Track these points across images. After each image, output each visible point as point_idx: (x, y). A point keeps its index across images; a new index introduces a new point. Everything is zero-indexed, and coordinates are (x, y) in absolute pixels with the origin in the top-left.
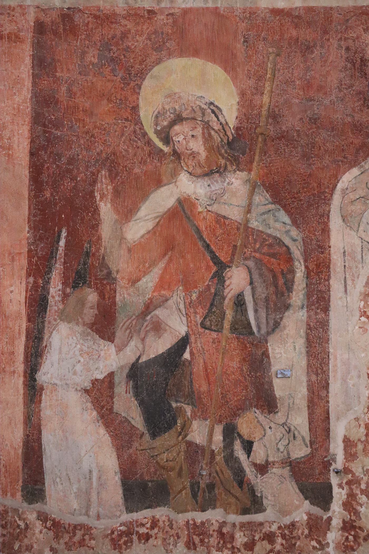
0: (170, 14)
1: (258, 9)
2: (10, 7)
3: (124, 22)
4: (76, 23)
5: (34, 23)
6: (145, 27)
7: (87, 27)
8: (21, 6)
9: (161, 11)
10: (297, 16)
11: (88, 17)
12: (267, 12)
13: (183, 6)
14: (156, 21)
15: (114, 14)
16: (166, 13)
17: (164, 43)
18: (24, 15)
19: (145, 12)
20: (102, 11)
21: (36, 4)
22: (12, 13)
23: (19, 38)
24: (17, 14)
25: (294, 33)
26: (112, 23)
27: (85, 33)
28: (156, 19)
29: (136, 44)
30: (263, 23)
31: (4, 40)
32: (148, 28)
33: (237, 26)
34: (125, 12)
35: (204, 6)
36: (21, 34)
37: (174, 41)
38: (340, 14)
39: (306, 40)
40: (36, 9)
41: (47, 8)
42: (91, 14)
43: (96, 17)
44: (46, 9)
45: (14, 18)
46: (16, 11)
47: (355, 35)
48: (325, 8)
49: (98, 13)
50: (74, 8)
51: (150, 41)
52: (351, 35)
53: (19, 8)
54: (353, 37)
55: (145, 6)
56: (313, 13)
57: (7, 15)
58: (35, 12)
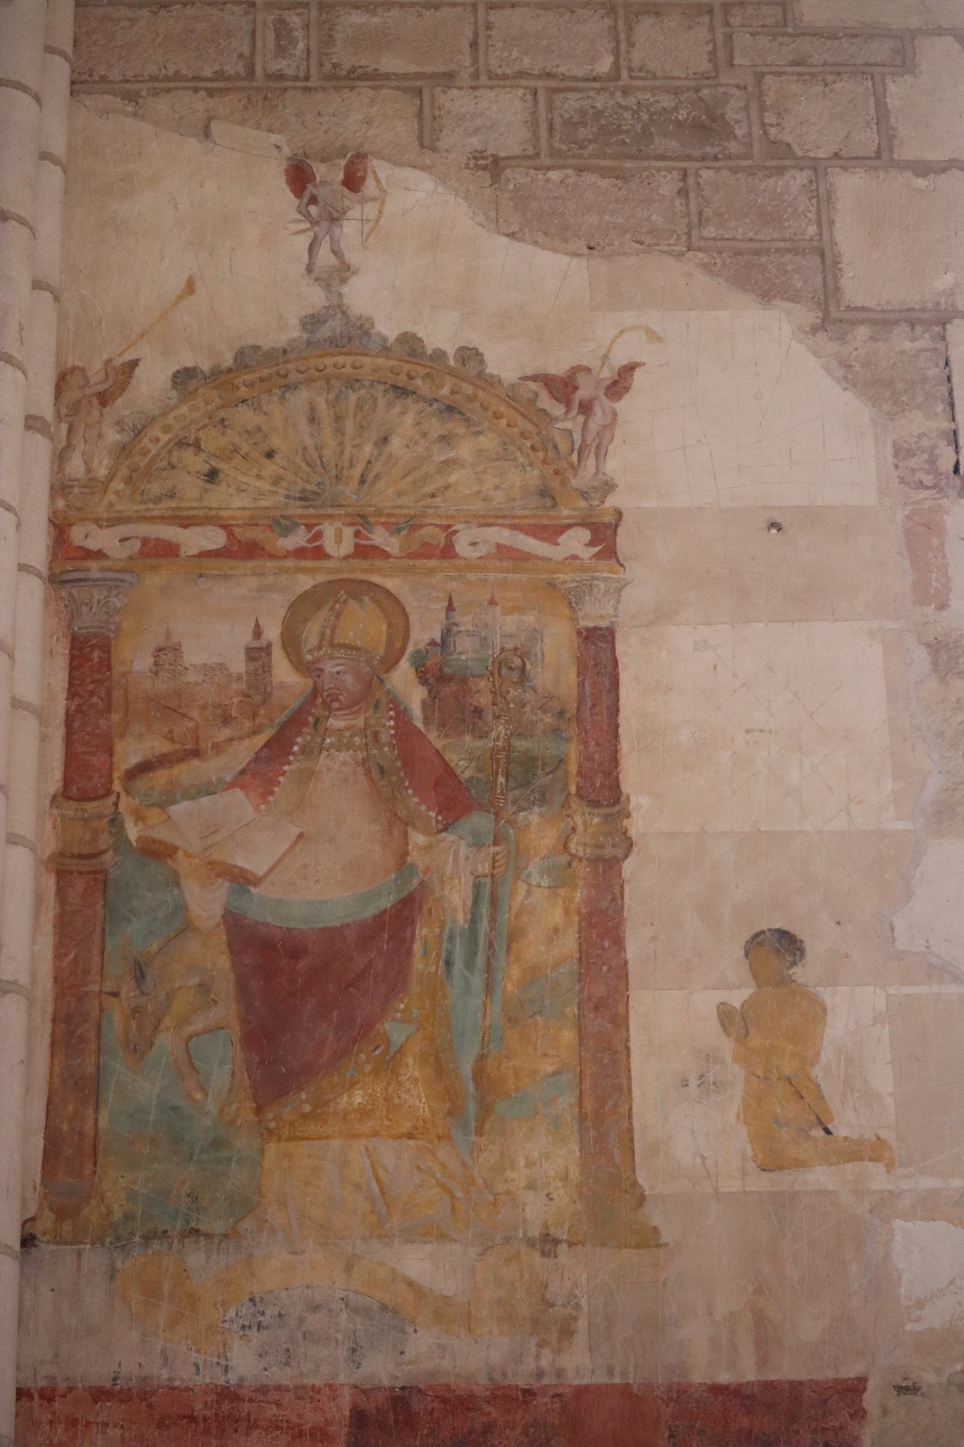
0: (557, 1395)
1: (689, 1385)
2: (313, 1387)
3: (487, 1408)
4: (413, 1411)
5: (350, 1411)
6: (519, 1416)
7: (431, 1416)
8: (330, 1386)
9: (544, 1390)
10: (749, 1395)
11: (433, 1401)
12: (703, 1391)
13: (577, 1382)
14: (536, 1406)
15: (472, 1397)
16: (551, 1394)
17: (548, 1440)
18: (334, 1399)
19: (519, 1393)
20: (454, 1391)
21: (352, 1382)
22: (318, 1397)
23: (328, 1435)
24: (324, 1399)
25: (745, 1422)
26: (468, 1409)
27: (428, 1426)
28: (535, 1403)
29: (505, 1442)
30: (698, 1407)
31: (304, 1440)
32: (523, 1418)
33: (659, 1412)
34: (488, 1393)
35: (609, 1382)
36: (331, 1429)
37: (563, 1437)
38: (814, 1392)
39: (764, 1434)
40: (354, 1389)
41: (369, 1387)
42: (436, 1396)
43: (444, 1401)
44: (367, 1390)
45: (320, 1404)
46: (322, 1392)
47: (837, 1424)
48: (791, 1383)
49: (447, 1395)
50: (411, 1387)
51: (527, 1437)
52: (831, 1424)
53: (327, 1388)
54: (833, 1426)
55: (519, 1384)
56: (774, 1391)
57: (309, 1401)
58: (351, 1395)
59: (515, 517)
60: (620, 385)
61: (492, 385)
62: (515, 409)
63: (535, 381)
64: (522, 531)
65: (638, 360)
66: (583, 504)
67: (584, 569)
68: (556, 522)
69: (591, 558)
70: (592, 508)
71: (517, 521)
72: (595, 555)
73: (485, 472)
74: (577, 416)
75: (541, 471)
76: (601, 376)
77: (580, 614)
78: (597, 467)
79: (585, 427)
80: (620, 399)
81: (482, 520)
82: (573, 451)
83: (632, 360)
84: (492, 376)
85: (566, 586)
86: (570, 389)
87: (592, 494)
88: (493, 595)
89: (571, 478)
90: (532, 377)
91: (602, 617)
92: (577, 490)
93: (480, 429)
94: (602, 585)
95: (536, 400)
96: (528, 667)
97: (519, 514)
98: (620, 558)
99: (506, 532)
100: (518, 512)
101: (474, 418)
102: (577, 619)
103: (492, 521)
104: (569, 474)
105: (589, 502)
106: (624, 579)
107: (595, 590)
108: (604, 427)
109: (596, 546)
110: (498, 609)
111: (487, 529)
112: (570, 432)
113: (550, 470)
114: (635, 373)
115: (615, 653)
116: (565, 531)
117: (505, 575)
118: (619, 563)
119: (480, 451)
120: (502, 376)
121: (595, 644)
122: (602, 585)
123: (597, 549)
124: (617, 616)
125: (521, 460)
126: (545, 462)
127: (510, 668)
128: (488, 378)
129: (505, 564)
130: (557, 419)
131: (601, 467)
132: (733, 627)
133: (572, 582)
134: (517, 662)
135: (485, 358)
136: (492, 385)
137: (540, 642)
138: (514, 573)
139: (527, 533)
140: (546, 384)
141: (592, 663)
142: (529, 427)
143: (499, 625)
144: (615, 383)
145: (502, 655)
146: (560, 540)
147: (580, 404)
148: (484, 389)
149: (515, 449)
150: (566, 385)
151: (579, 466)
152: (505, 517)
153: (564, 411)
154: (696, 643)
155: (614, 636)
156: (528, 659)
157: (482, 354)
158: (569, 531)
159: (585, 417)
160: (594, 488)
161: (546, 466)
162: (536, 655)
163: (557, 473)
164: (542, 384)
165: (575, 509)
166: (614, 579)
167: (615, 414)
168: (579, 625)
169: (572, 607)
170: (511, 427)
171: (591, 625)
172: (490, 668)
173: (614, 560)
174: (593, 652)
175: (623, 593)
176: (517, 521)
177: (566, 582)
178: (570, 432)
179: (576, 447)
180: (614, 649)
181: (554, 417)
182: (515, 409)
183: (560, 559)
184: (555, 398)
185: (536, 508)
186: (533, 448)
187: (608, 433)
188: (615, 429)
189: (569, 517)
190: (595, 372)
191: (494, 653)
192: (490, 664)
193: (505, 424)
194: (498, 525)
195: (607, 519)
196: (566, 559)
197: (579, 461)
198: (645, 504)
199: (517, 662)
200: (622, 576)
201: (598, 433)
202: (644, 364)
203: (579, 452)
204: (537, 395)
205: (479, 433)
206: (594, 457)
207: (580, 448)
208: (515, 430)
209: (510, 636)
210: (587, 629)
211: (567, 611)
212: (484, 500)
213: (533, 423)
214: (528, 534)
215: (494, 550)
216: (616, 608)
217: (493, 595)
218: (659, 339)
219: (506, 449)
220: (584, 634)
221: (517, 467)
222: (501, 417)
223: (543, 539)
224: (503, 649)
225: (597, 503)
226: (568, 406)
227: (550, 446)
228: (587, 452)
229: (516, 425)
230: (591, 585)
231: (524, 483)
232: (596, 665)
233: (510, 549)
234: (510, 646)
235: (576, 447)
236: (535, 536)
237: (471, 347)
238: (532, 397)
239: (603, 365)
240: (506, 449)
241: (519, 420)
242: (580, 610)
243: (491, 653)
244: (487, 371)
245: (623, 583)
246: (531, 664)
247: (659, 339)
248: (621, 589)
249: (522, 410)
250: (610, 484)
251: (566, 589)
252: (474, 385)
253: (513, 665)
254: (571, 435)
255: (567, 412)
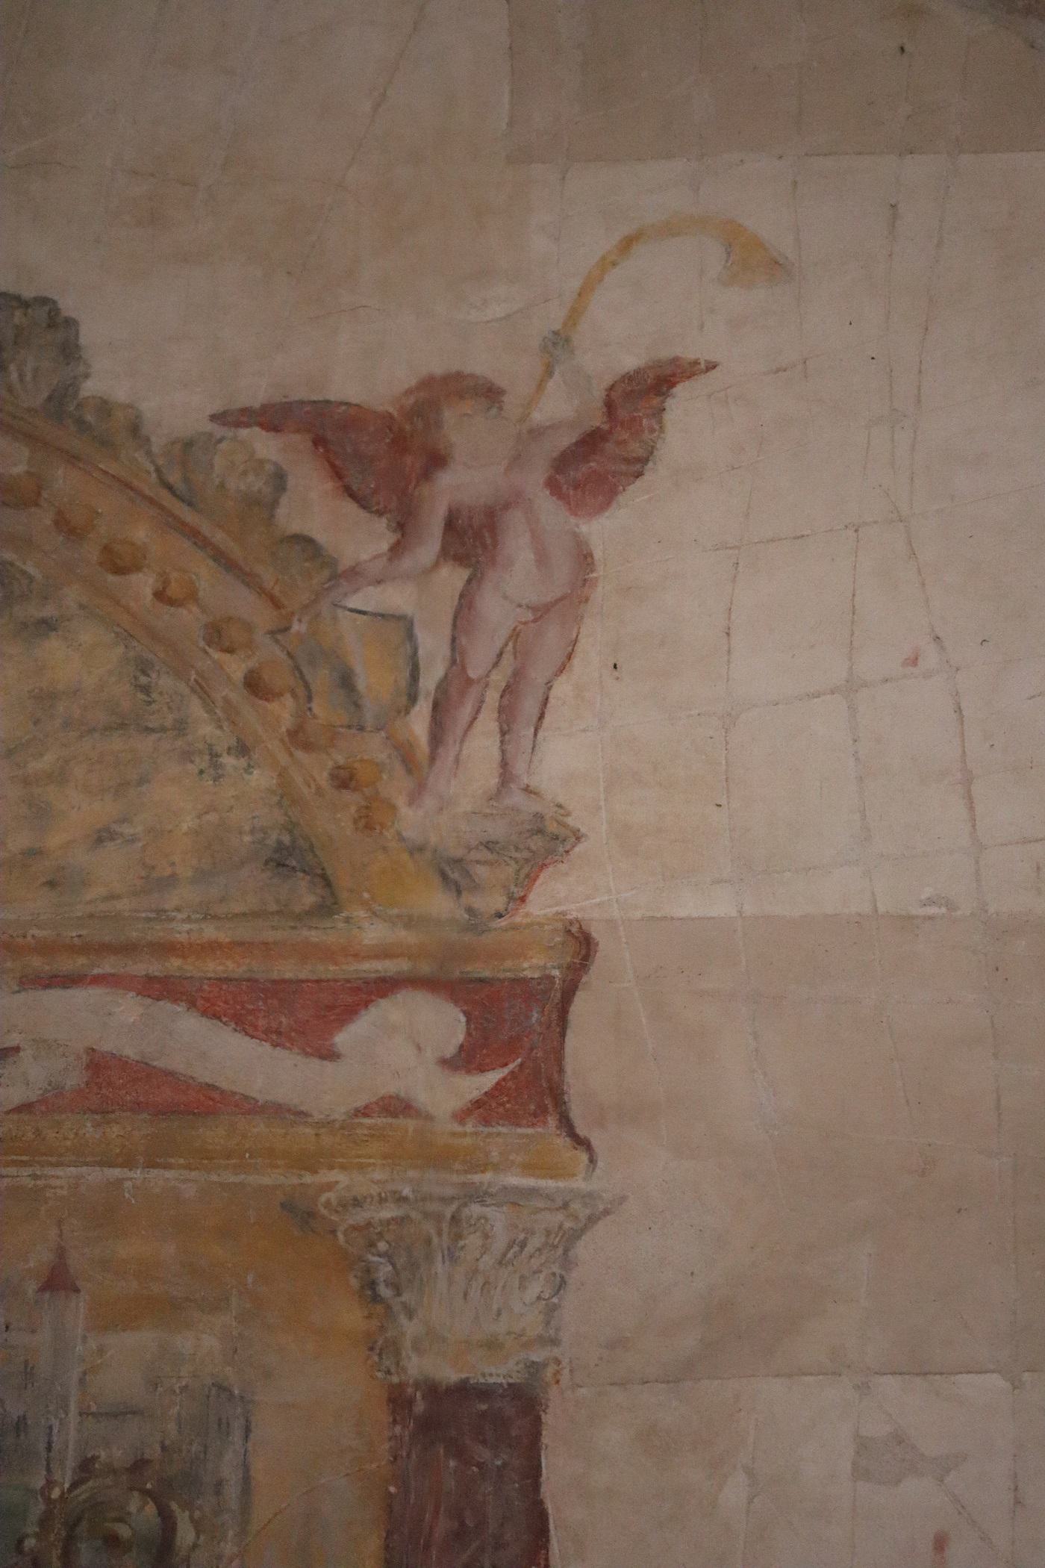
59: (167, 949)
60: (610, 447)
61: (105, 443)
62: (194, 535)
63: (273, 427)
64: (192, 1004)
65: (690, 350)
66: (440, 904)
67: (439, 1158)
68: (328, 970)
69: (461, 1117)
70: (475, 922)
71: (174, 964)
72: (478, 1104)
73: (59, 776)
74: (436, 565)
75: (282, 774)
76: (537, 417)
77: (410, 1328)
78: (504, 764)
79: (465, 606)
80: (606, 505)
81: (36, 962)
82: (413, 698)
83: (665, 353)
84: (105, 408)
85: (359, 1217)
86: (412, 462)
87: (481, 872)
88: (61, 1253)
89: (401, 801)
90: (265, 408)
91: (492, 1345)
92: (421, 849)
93: (49, 611)
94: (498, 1219)
95: (275, 503)
96: (185, 1534)
97: (182, 938)
98: (576, 1114)
99: (129, 1008)
100: (181, 931)
101: (31, 569)
102: (394, 1348)
103: (68, 964)
104: (395, 786)
105: (468, 899)
106: (589, 1197)
107: (473, 1241)
108: (541, 612)
109: (482, 1069)
110: (77, 1310)
111: (54, 998)
112: (405, 625)
113: (317, 768)
114: (670, 403)
115: (536, 1486)
116: (366, 1004)
117: (116, 1173)
118: (573, 1135)
119: (46, 698)
120: (148, 407)
121: (459, 1452)
122: (498, 1219)
123: (491, 1079)
124: (554, 1342)
125: (206, 730)
126: (298, 738)
127: (112, 1541)
128: (89, 418)
129: (115, 1131)
130: (354, 574)
131: (519, 767)
132: (1016, 1385)
133: (382, 1200)
134: (143, 1514)
135: (83, 341)
136: (105, 443)
137: (237, 1436)
138: (151, 1165)
139: (210, 1013)
140: (318, 441)
141: (443, 1526)
142: (243, 603)
143: (75, 1374)
144: (591, 442)
145: (83, 1492)
146: (342, 1039)
147: (451, 525)
148: (73, 459)
149: (183, 688)
150: (400, 443)
151: (433, 758)
152: (128, 949)
153: (385, 546)
154: (863, 1445)
155: (537, 1422)
156: (188, 1506)
157: (70, 323)
158: (383, 1003)
159: (464, 574)
160: (489, 845)
161: (299, 754)
162: (219, 1486)
163: (344, 780)
164: (301, 441)
165: (410, 922)
166: (549, 1197)
167: (584, 559)
168: (404, 1370)
169: (376, 1298)
170: (171, 602)
171: (449, 1374)
172: (30, 1543)
173: (552, 1121)
174: (450, 1483)
175: (582, 1250)
176: (174, 964)
177: (357, 1203)
178: (405, 625)
179: (428, 683)
180: (533, 1473)
181: (345, 563)
182: (194, 535)
183: (339, 1114)
184: (353, 496)
185: (256, 915)
186: (254, 685)
187: (553, 636)
188: (579, 619)
189: (384, 953)
190: (511, 402)
191: (50, 1484)
192: (32, 1529)
193: (148, 592)
194: (98, 980)
195: (533, 966)
196: (365, 1112)
197: (437, 737)
198: (687, 904)
199: (143, 1514)
200: (579, 1184)
201: (515, 635)
202: (712, 366)
203: (436, 706)
204: (279, 480)
205: (47, 626)
206: (494, 726)
207: (443, 687)
208: (189, 619)
209: (121, 1413)
210: (433, 1390)
211: (352, 1317)
212: (52, 884)
213: (262, 591)
214: (216, 1016)
215: (75, 1079)
216: (551, 1310)
217: (61, 1253)
218: (776, 268)
219: (146, 689)
220: (420, 1407)
221: (187, 756)
222: (137, 568)
223: (276, 1037)
224: (86, 1467)
225: (499, 902)
226: (405, 526)
227: (321, 678)
228: (466, 711)
229: (192, 596)
230: (455, 1219)
231: (212, 817)
232: (460, 1535)
233: (143, 1073)
234: (118, 1454)
235: (428, 683)
236: (242, 1022)
237: (28, 293)
238: (256, 484)
239: (549, 372)
240: (146, 689)
241: (204, 574)
242: (410, 1314)
243: (39, 1483)
244: (90, 388)
245: (584, 1213)
246: (197, 1525)
247: (776, 268)
248: (576, 1235)
249: (219, 537)
250: (552, 827)
251: (354, 1228)
252: (30, 438)
253: (124, 1531)
254: (410, 636)
255: (397, 550)
